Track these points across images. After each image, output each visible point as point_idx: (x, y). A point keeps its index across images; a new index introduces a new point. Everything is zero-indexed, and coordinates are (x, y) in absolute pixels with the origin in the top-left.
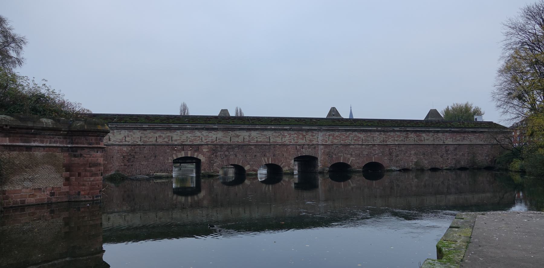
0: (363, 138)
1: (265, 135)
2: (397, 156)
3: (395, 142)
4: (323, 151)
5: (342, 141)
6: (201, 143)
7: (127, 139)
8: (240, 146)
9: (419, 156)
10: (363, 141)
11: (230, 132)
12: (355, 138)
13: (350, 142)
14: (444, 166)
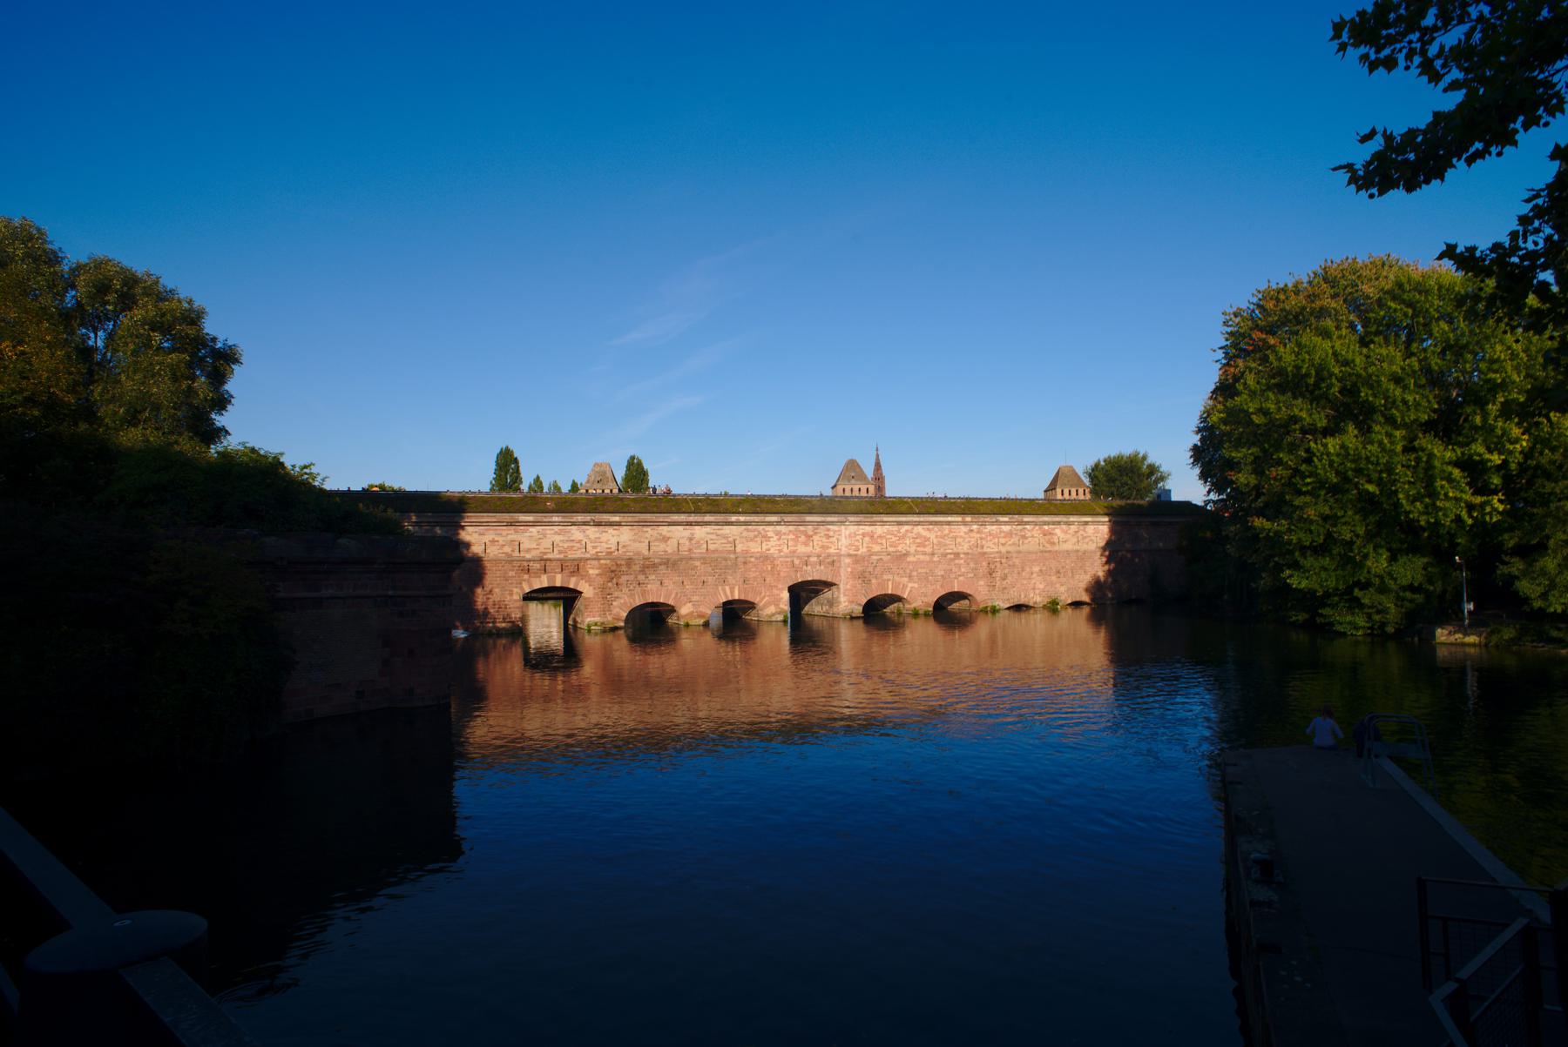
0: (935, 541)
1: (726, 537)
4: (849, 570)
5: (891, 546)
6: (583, 556)
8: (670, 563)
9: (1048, 578)
10: (935, 547)
11: (649, 529)
12: (918, 541)
13: (908, 549)
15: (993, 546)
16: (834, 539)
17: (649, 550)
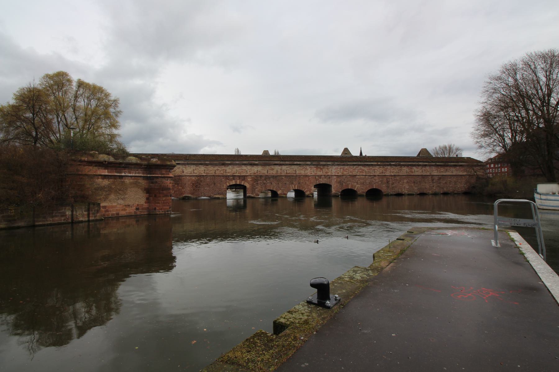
0: (367, 171)
1: (293, 169)
2: (393, 184)
3: (391, 173)
4: (335, 180)
7: (195, 171)
8: (274, 177)
9: (410, 184)
11: (267, 166)
12: (360, 171)
13: (357, 173)
14: (430, 192)
15: (389, 173)
16: (330, 170)
17: (267, 172)
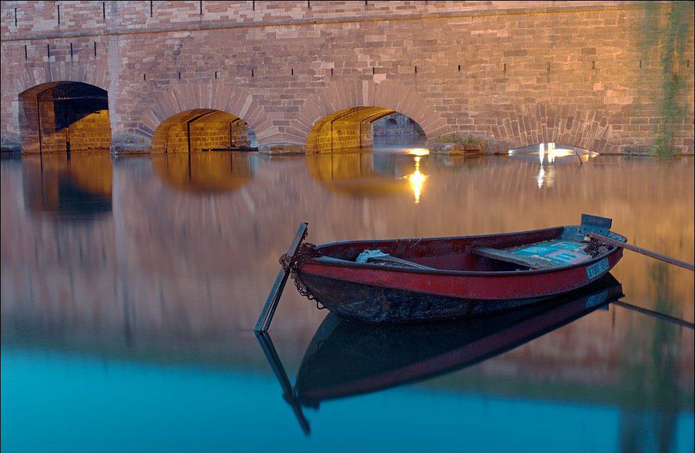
4: (125, 61)
13: (250, 14)
